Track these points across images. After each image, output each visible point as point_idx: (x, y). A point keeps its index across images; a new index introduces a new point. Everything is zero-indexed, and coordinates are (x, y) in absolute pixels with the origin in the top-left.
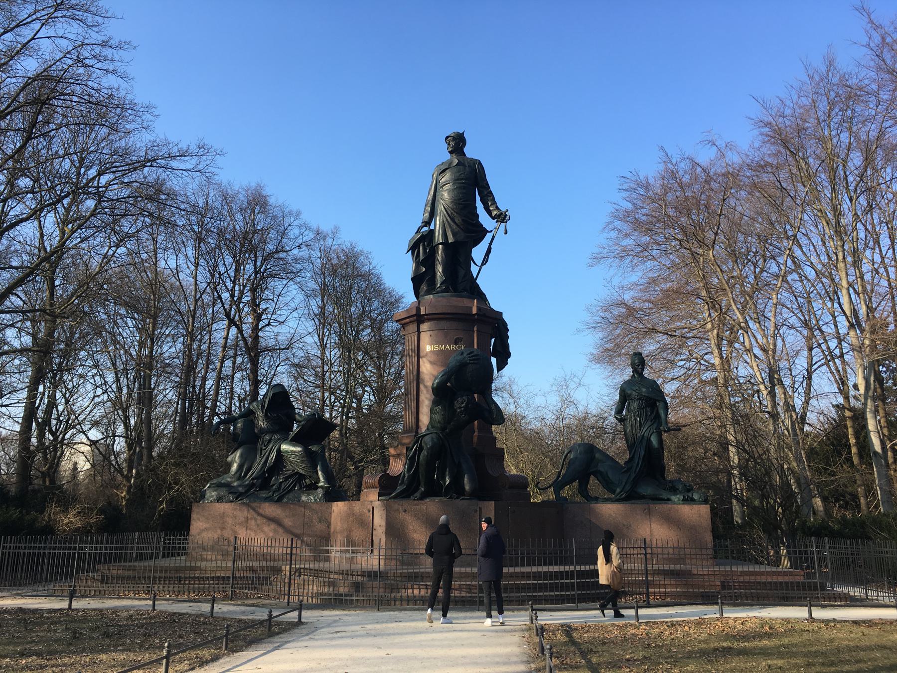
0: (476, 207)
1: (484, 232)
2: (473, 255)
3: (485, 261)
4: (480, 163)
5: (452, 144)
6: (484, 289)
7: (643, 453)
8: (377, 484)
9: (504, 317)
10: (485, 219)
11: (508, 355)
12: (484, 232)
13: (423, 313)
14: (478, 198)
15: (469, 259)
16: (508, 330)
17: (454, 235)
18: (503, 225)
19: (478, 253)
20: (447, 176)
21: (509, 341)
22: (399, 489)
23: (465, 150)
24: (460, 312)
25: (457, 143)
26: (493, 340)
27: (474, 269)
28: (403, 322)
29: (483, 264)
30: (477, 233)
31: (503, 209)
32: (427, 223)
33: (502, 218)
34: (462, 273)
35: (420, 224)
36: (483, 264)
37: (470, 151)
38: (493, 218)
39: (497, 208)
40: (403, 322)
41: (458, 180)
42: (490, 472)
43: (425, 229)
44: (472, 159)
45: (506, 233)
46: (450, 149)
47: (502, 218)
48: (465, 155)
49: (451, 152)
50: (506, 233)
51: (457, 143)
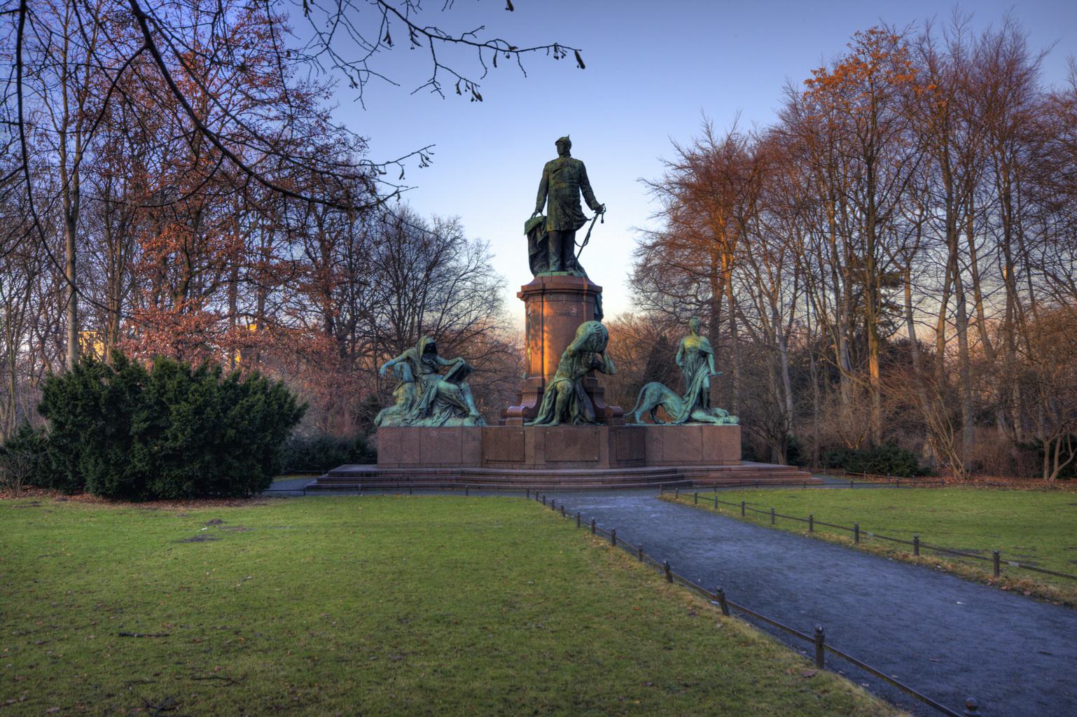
1: (586, 220)
5: (562, 147)
7: (697, 391)
10: (587, 212)
12: (586, 220)
13: (547, 287)
18: (600, 216)
19: (580, 235)
22: (540, 418)
25: (564, 146)
27: (577, 250)
29: (583, 245)
31: (601, 204)
36: (583, 245)
37: (575, 153)
44: (576, 161)
45: (602, 222)
47: (599, 209)
49: (560, 155)
50: (602, 222)
51: (564, 146)
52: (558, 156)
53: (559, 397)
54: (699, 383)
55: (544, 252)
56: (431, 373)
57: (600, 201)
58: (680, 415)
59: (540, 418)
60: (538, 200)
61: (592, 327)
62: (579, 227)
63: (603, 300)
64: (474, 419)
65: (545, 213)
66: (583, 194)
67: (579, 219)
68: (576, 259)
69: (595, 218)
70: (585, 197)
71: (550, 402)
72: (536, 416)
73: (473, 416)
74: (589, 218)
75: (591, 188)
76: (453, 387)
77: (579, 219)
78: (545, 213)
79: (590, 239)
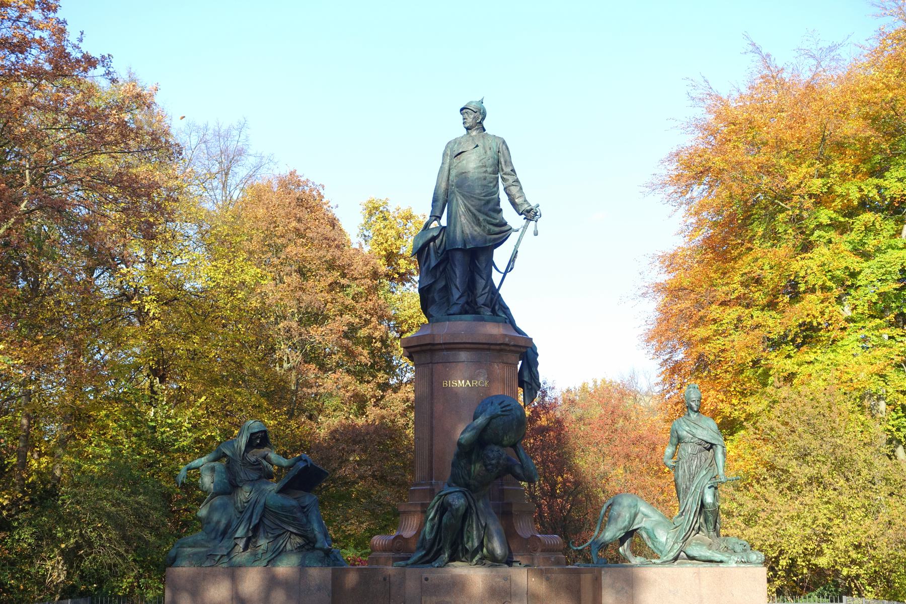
3: (509, 268)
4: (504, 142)
9: (534, 341)
10: (509, 215)
15: (491, 263)
16: (537, 355)
18: (532, 223)
19: (501, 256)
21: (539, 369)
23: (485, 124)
24: (484, 341)
26: (520, 362)
27: (496, 277)
28: (412, 350)
29: (506, 272)
31: (533, 204)
34: (481, 283)
36: (506, 272)
38: (521, 214)
40: (412, 350)
43: (435, 224)
45: (536, 234)
47: (530, 214)
48: (484, 130)
50: (536, 234)
52: (465, 131)
55: (442, 284)
56: (260, 478)
57: (532, 196)
58: (668, 548)
60: (435, 200)
63: (538, 359)
64: (322, 554)
66: (505, 189)
67: (497, 229)
69: (525, 227)
70: (508, 195)
71: (432, 527)
73: (321, 549)
74: (514, 227)
75: (517, 181)
76: (289, 502)
77: (497, 229)
78: (444, 222)
79: (517, 260)
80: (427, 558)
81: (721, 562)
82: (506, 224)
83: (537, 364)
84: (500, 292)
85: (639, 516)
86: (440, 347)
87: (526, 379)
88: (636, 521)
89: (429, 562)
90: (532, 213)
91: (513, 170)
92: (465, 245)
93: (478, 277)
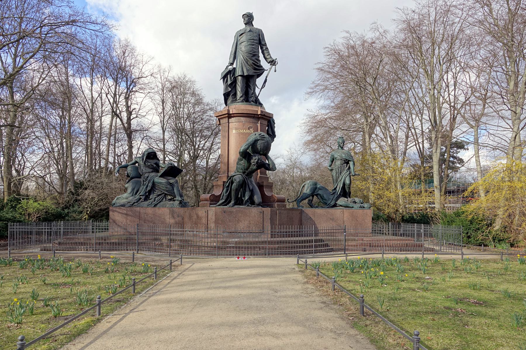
0: (259, 57)
2: (257, 83)
3: (263, 86)
4: (262, 31)
5: (246, 19)
6: (262, 102)
7: (341, 186)
8: (209, 199)
10: (264, 63)
11: (275, 136)
13: (231, 112)
14: (260, 51)
15: (255, 85)
17: (248, 70)
18: (274, 66)
19: (259, 81)
20: (244, 38)
21: (276, 129)
22: (221, 202)
23: (253, 23)
24: (252, 113)
25: (249, 19)
27: (257, 91)
29: (262, 88)
30: (258, 70)
31: (274, 58)
32: (232, 64)
33: (273, 63)
35: (227, 64)
36: (262, 88)
37: (256, 24)
38: (269, 63)
39: (271, 57)
41: (250, 40)
42: (266, 193)
43: (230, 67)
44: (257, 29)
45: (275, 71)
46: (245, 22)
47: (273, 63)
48: (253, 26)
49: (246, 24)
50: (275, 71)
51: (249, 19)
53: (234, 184)
54: (342, 180)
59: (221, 202)
61: (257, 135)
62: (259, 76)
65: (234, 66)
68: (257, 98)
69: (271, 69)
72: (218, 202)
75: (267, 48)
80: (225, 204)
81: (353, 207)
82: (262, 67)
83: (275, 127)
84: (259, 98)
85: (317, 189)
86: (232, 115)
87: (270, 133)
88: (316, 191)
89: (226, 205)
90: (274, 62)
91: (266, 43)
92: (244, 74)
93: (249, 89)
